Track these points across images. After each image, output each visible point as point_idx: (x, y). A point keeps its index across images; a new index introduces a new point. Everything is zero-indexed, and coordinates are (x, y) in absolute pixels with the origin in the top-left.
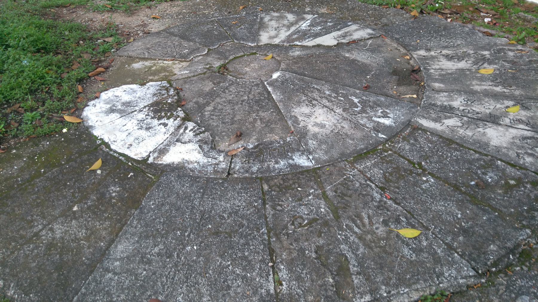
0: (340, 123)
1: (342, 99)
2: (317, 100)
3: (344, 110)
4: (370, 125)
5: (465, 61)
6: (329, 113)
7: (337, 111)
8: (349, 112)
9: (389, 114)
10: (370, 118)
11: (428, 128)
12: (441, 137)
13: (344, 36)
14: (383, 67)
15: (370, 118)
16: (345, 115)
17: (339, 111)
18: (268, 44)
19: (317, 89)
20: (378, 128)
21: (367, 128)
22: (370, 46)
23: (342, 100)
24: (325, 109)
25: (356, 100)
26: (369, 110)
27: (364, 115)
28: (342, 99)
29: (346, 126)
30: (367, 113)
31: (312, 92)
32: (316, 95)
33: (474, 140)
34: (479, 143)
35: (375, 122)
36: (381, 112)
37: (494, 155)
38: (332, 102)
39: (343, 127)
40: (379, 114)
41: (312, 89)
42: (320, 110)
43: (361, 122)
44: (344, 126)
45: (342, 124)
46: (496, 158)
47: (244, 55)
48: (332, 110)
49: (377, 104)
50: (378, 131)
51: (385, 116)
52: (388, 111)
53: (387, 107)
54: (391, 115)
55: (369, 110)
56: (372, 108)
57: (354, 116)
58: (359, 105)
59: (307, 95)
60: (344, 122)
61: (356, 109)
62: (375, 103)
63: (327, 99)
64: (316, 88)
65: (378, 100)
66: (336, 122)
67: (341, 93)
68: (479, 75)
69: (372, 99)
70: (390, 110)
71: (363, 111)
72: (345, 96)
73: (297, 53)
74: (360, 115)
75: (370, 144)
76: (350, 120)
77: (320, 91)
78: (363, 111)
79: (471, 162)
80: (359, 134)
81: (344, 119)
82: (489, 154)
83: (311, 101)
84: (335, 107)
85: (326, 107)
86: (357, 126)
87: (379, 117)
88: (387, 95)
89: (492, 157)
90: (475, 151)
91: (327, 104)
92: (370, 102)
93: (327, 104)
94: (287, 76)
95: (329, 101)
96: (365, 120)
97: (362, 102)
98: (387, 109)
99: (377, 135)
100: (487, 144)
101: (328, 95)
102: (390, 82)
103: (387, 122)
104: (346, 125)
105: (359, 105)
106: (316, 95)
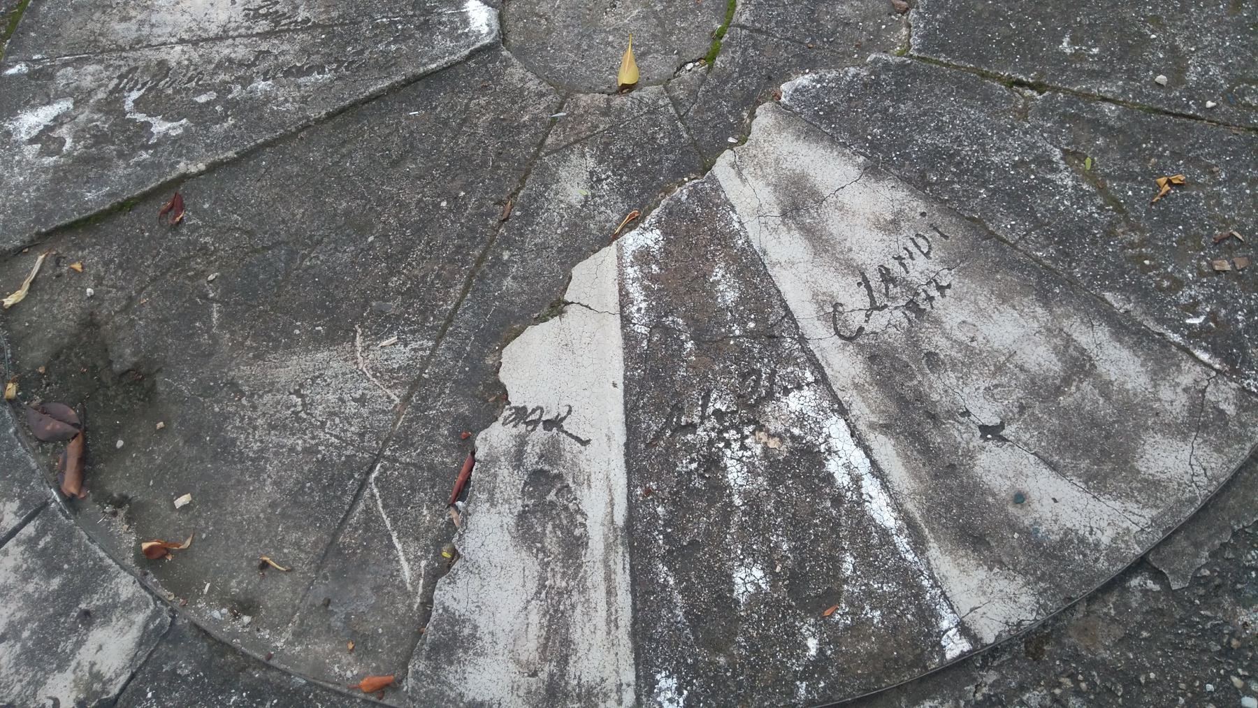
0: (142, 23)
1: (202, 99)
2: (264, 36)
3: (162, 64)
4: (65, 76)
6: (194, 25)
7: (178, 48)
8: (147, 68)
9: (41, 154)
10: (81, 97)
13: (547, 487)
14: (207, 391)
15: (81, 97)
16: (147, 52)
17: (174, 55)
18: (742, 141)
19: (301, 72)
20: (38, 87)
21: (65, 64)
22: (370, 517)
23: (199, 92)
24: (214, 30)
25: (160, 127)
26: (102, 122)
27: (101, 95)
28: (202, 99)
29: (119, 27)
30: (98, 108)
31: (304, 50)
32: (287, 50)
35: (60, 96)
36: (62, 142)
38: (219, 66)
39: (125, 19)
40: (64, 131)
41: (317, 59)
42: (223, 17)
43: (91, 68)
44: (124, 25)
45: (133, 25)
47: (728, 23)
48: (195, 44)
49: (90, 163)
50: (30, 75)
51: (45, 138)
52: (48, 161)
53: (60, 176)
54: (31, 151)
55: (102, 122)
56: (100, 138)
57: (124, 69)
58: (141, 117)
59: (306, 26)
60: (134, 35)
61: (135, 95)
62: (102, 162)
63: (241, 64)
64: (308, 72)
65: (100, 181)
66: (154, 18)
67: (224, 118)
69: (121, 170)
70: (45, 170)
71: (112, 106)
72: (202, 116)
73: (573, 184)
74: (111, 86)
75: (30, 28)
76: (123, 50)
77: (287, 74)
78: (112, 106)
80: (71, 29)
81: (139, 41)
83: (277, 23)
84: (195, 56)
85: (218, 39)
86: (92, 49)
87: (58, 121)
88: (89, 224)
91: (224, 50)
92: (121, 155)
93: (224, 50)
94: (441, 42)
95: (230, 60)
96: (88, 82)
97: (137, 135)
98: (56, 167)
99: (29, 61)
101: (251, 81)
102: (125, 310)
103: (31, 120)
104: (123, 31)
105: (141, 117)
106: (287, 50)
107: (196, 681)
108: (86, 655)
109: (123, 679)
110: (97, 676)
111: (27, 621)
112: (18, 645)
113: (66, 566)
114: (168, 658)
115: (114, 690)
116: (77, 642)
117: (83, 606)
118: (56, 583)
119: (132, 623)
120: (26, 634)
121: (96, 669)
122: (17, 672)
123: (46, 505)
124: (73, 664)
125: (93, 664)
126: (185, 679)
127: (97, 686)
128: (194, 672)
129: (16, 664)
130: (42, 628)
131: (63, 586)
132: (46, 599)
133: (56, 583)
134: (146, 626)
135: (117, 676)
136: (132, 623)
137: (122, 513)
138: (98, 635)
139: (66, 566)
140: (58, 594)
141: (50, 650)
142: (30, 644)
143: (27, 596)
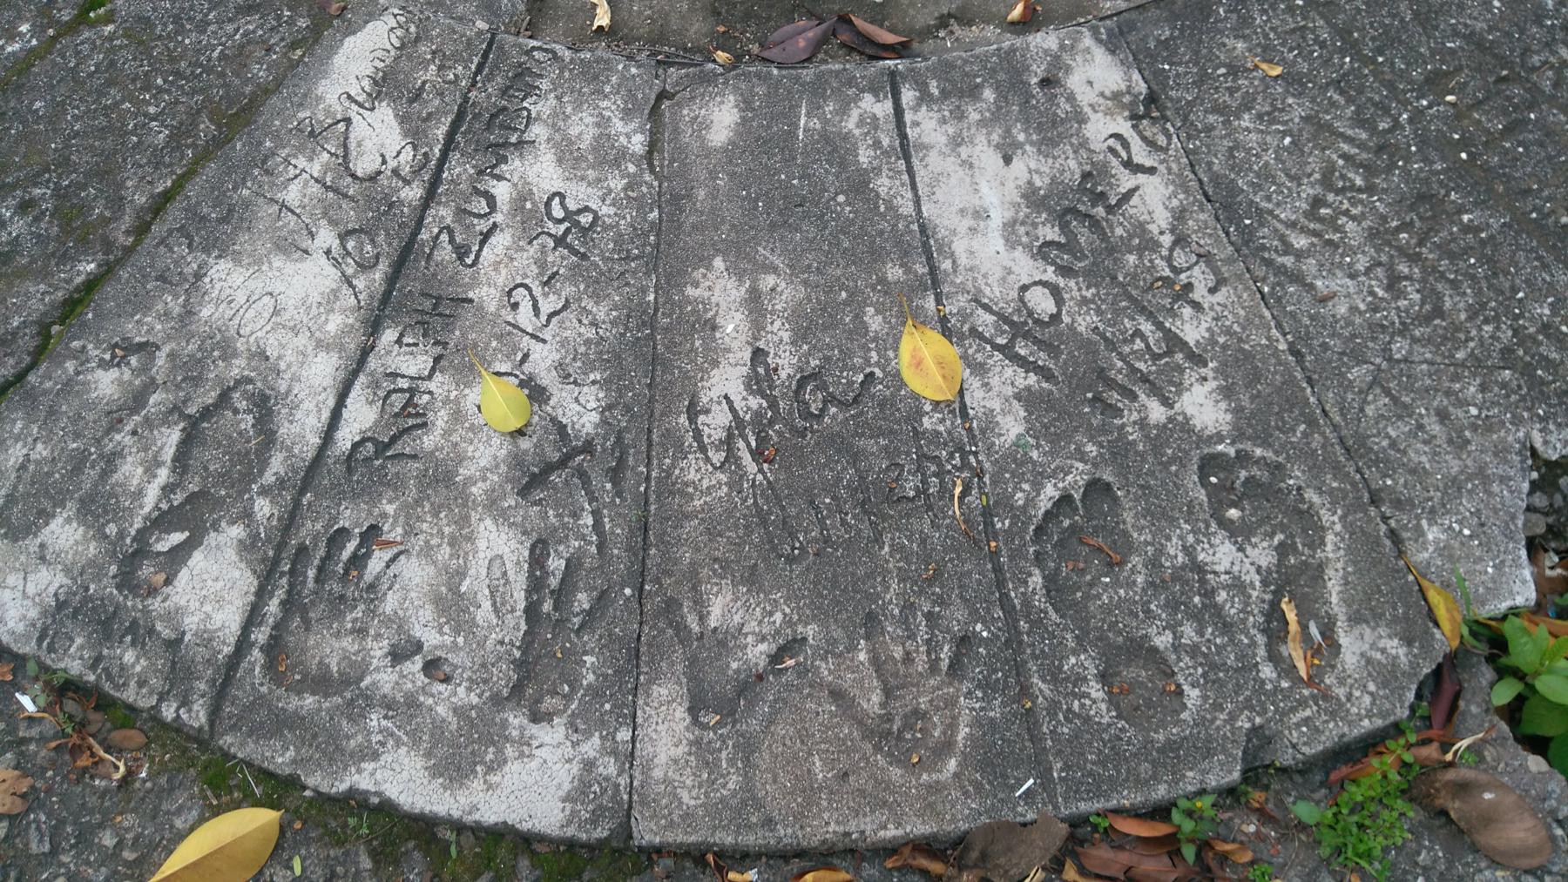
5: (1050, 274)
11: (333, 50)
12: (266, 91)
33: (247, 204)
34: (224, 220)
37: (144, 261)
46: (120, 262)
68: (874, 322)
79: (106, 173)
82: (149, 242)
89: (129, 251)
90: (167, 197)
100: (219, 246)
107: (1182, 30)
108: (1085, 97)
109: (1136, 76)
110: (1116, 96)
111: (1008, 131)
112: (1028, 147)
113: (978, 80)
114: (1144, 39)
115: (1142, 87)
116: (1068, 100)
117: (1034, 80)
118: (989, 94)
119: (1088, 50)
120: (1021, 137)
121: (1107, 93)
122: (1055, 158)
123: (893, 74)
124: (1087, 109)
125: (1102, 94)
126: (1172, 37)
127: (1127, 99)
128: (1173, 28)
129: (1046, 156)
130: (1027, 121)
131: (997, 88)
132: (999, 108)
133: (989, 94)
134: (1099, 41)
135: (1130, 80)
136: (1088, 50)
137: (956, 27)
138: (1075, 82)
139: (978, 80)
140: (1002, 96)
141: (1055, 122)
142: (1034, 137)
143: (982, 123)
